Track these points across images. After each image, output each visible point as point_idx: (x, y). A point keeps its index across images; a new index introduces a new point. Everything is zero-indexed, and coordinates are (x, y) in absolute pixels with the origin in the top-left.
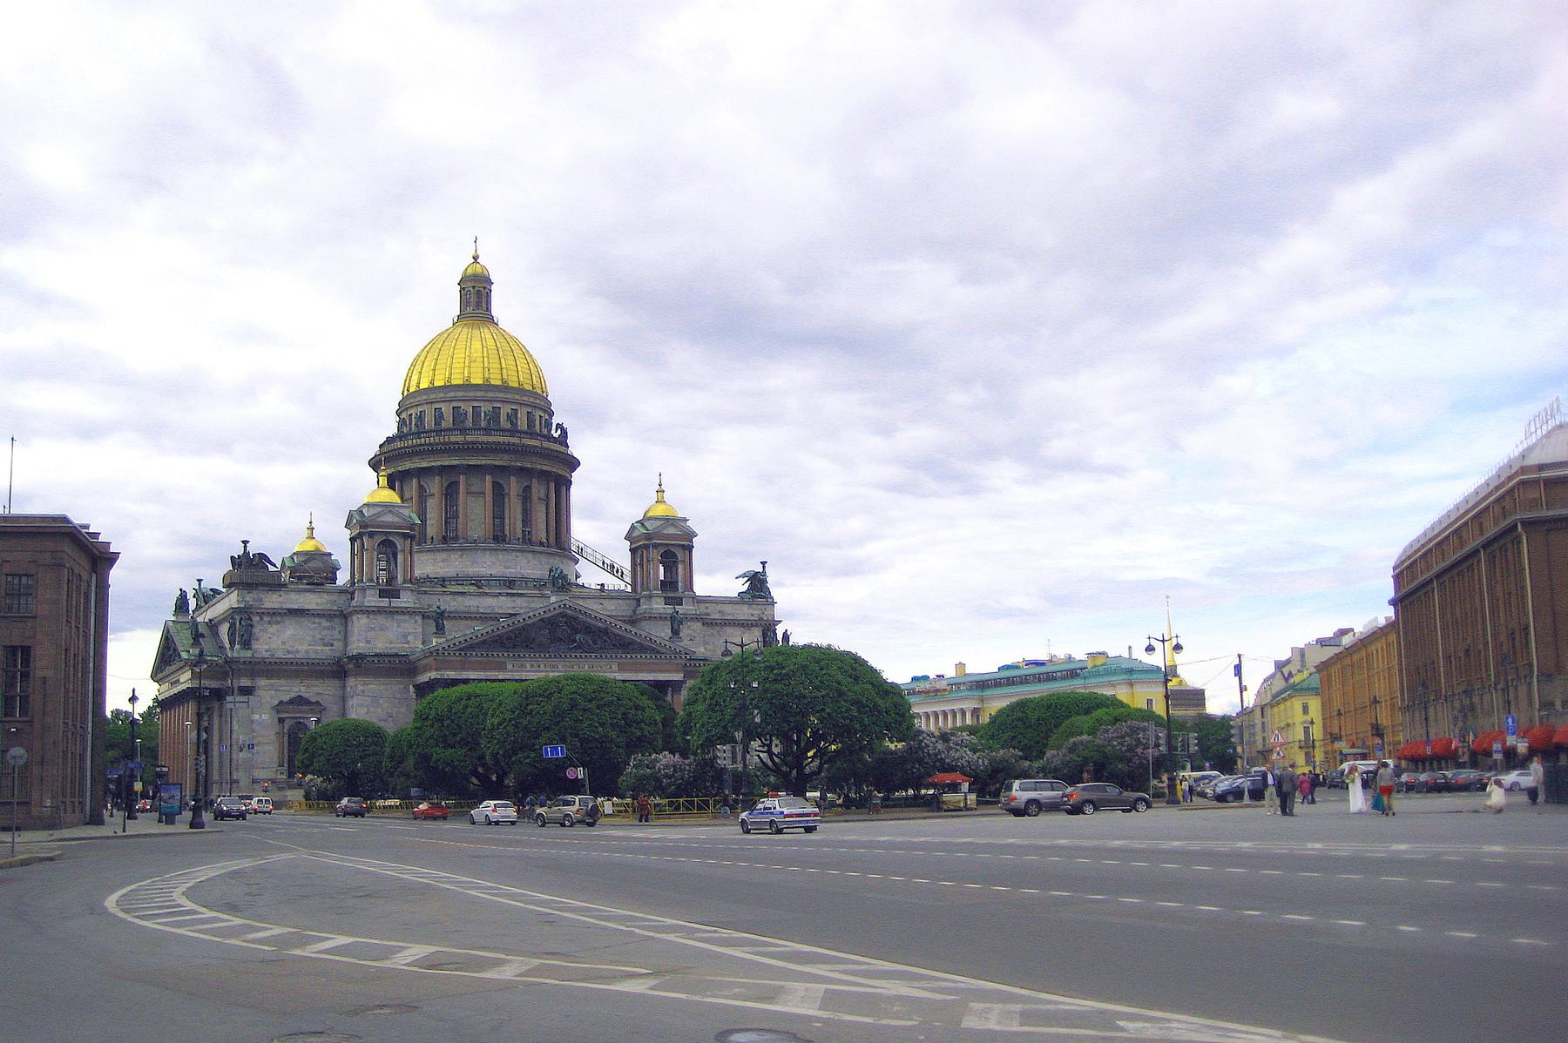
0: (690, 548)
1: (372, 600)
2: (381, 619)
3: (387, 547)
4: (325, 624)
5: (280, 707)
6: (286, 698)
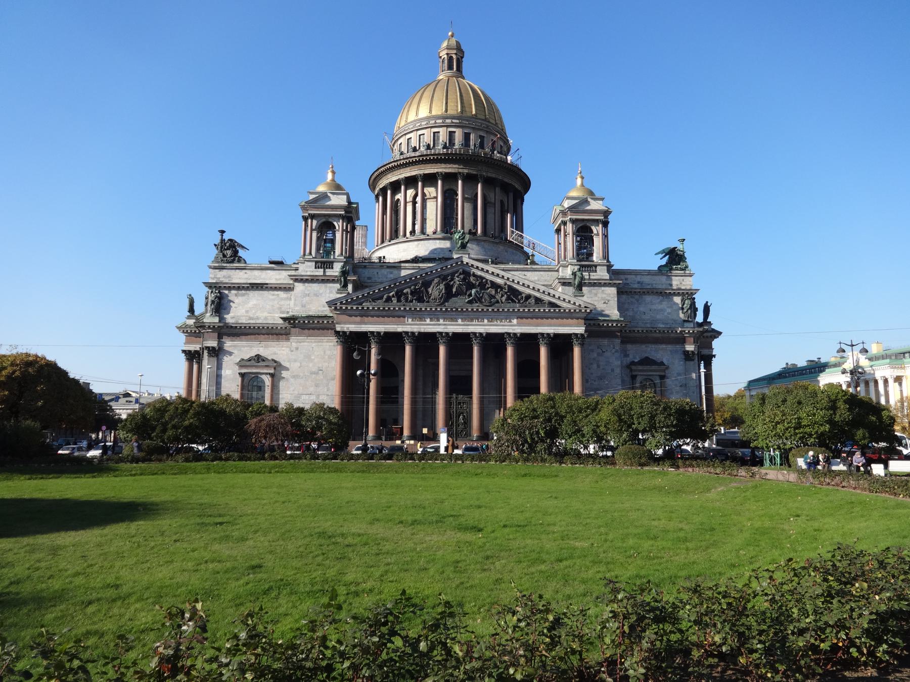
0: (605, 224)
1: (308, 269)
2: (315, 286)
3: (326, 226)
4: (282, 294)
5: (242, 363)
6: (246, 357)
